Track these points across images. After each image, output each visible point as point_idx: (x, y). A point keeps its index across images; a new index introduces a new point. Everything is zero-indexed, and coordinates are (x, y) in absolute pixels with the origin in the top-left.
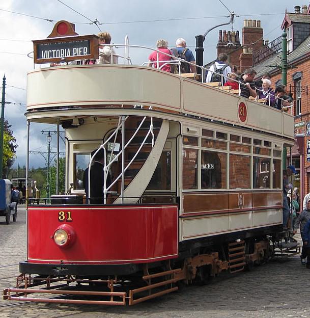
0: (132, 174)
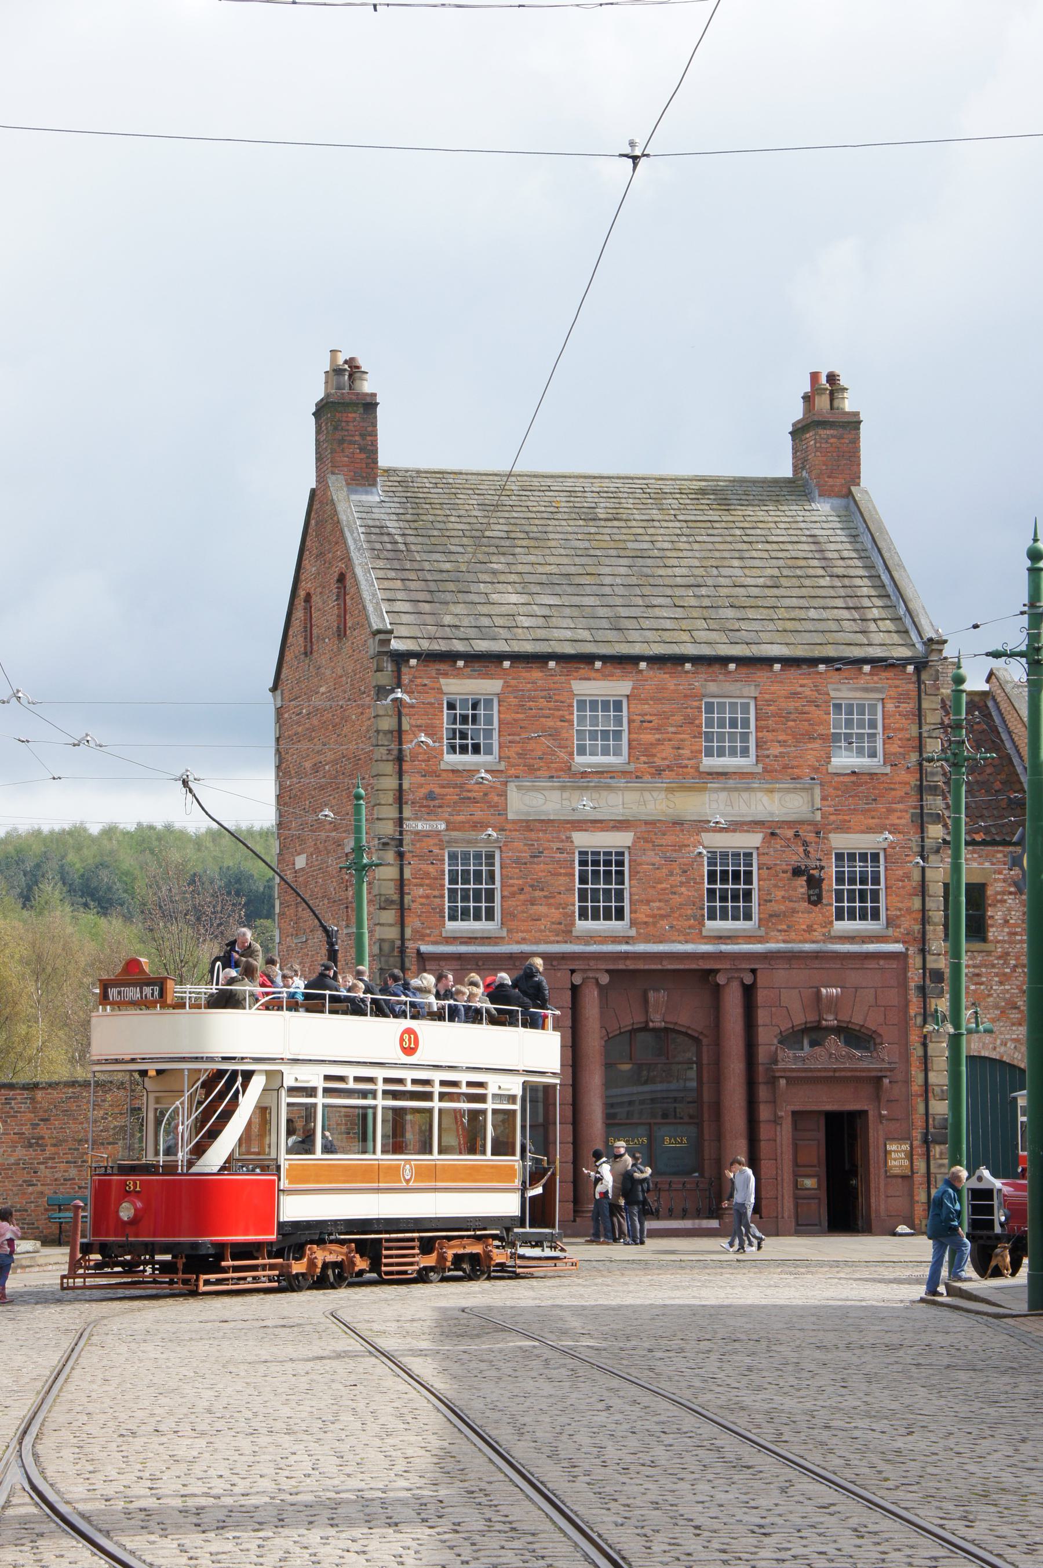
0: (213, 1134)
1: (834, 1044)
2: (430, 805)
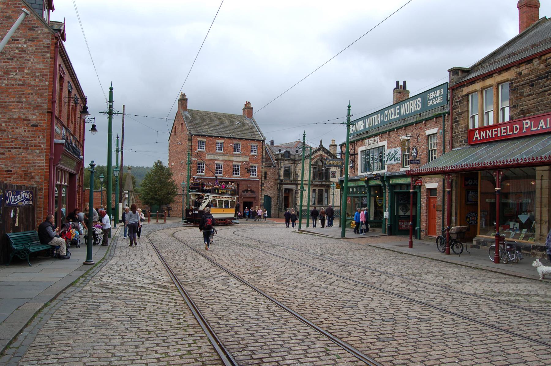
1: (249, 192)
2: (195, 157)
